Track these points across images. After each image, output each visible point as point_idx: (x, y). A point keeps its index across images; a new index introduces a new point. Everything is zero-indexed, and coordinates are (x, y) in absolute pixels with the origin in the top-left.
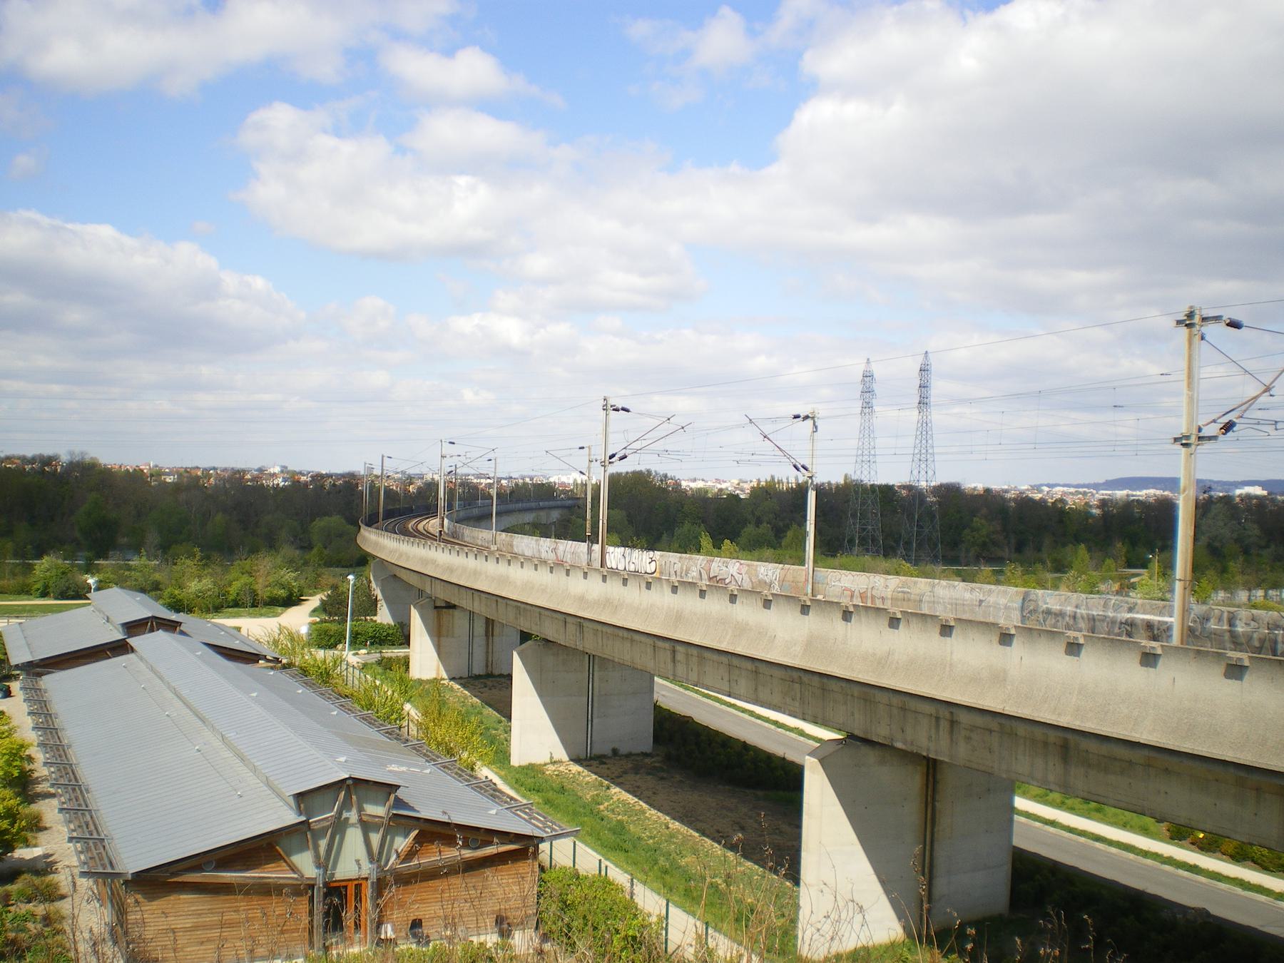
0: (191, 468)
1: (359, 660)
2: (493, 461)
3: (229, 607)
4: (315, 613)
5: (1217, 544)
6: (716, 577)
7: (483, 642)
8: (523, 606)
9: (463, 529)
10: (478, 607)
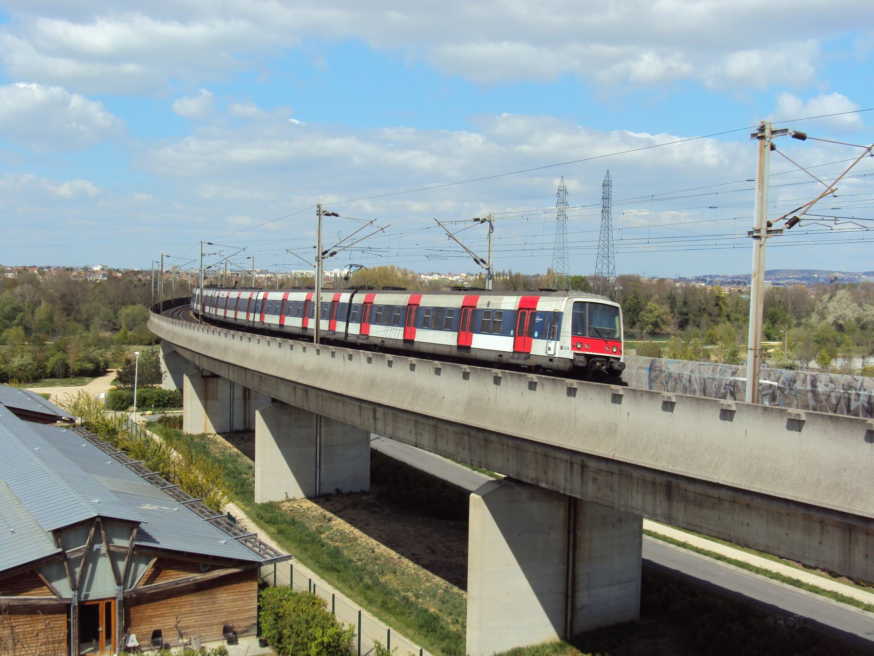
0: (29, 267)
1: (145, 419)
2: (252, 259)
3: (47, 378)
4: (116, 383)
5: (841, 322)
8: (263, 376)
10: (232, 376)
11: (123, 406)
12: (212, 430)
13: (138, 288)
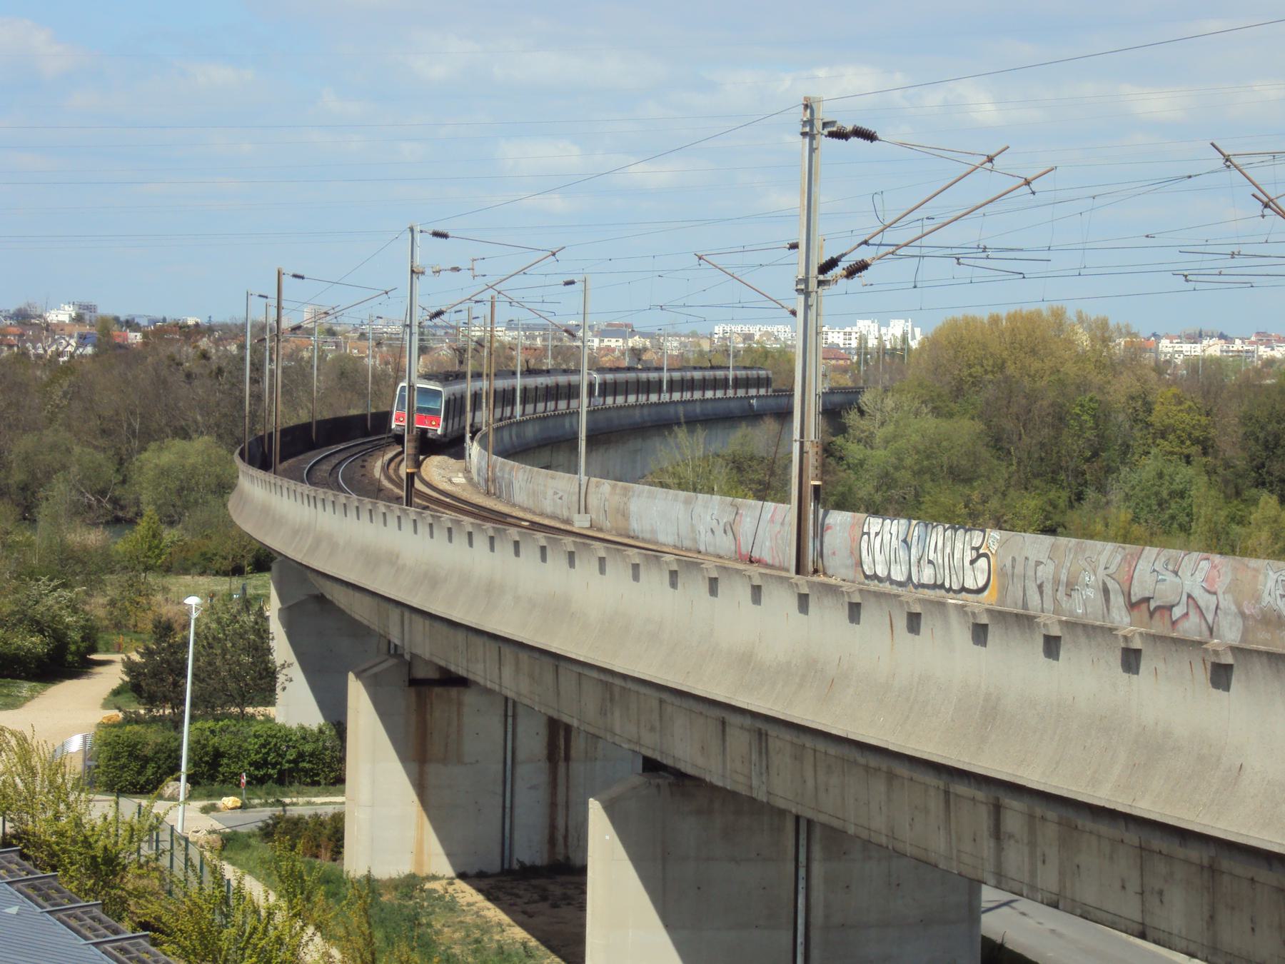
1: (218, 826)
2: (578, 286)
4: (121, 700)
6: (1147, 600)
7: (542, 778)
8: (618, 682)
9: (512, 469)
11: (142, 780)
12: (439, 864)
13: (196, 383)
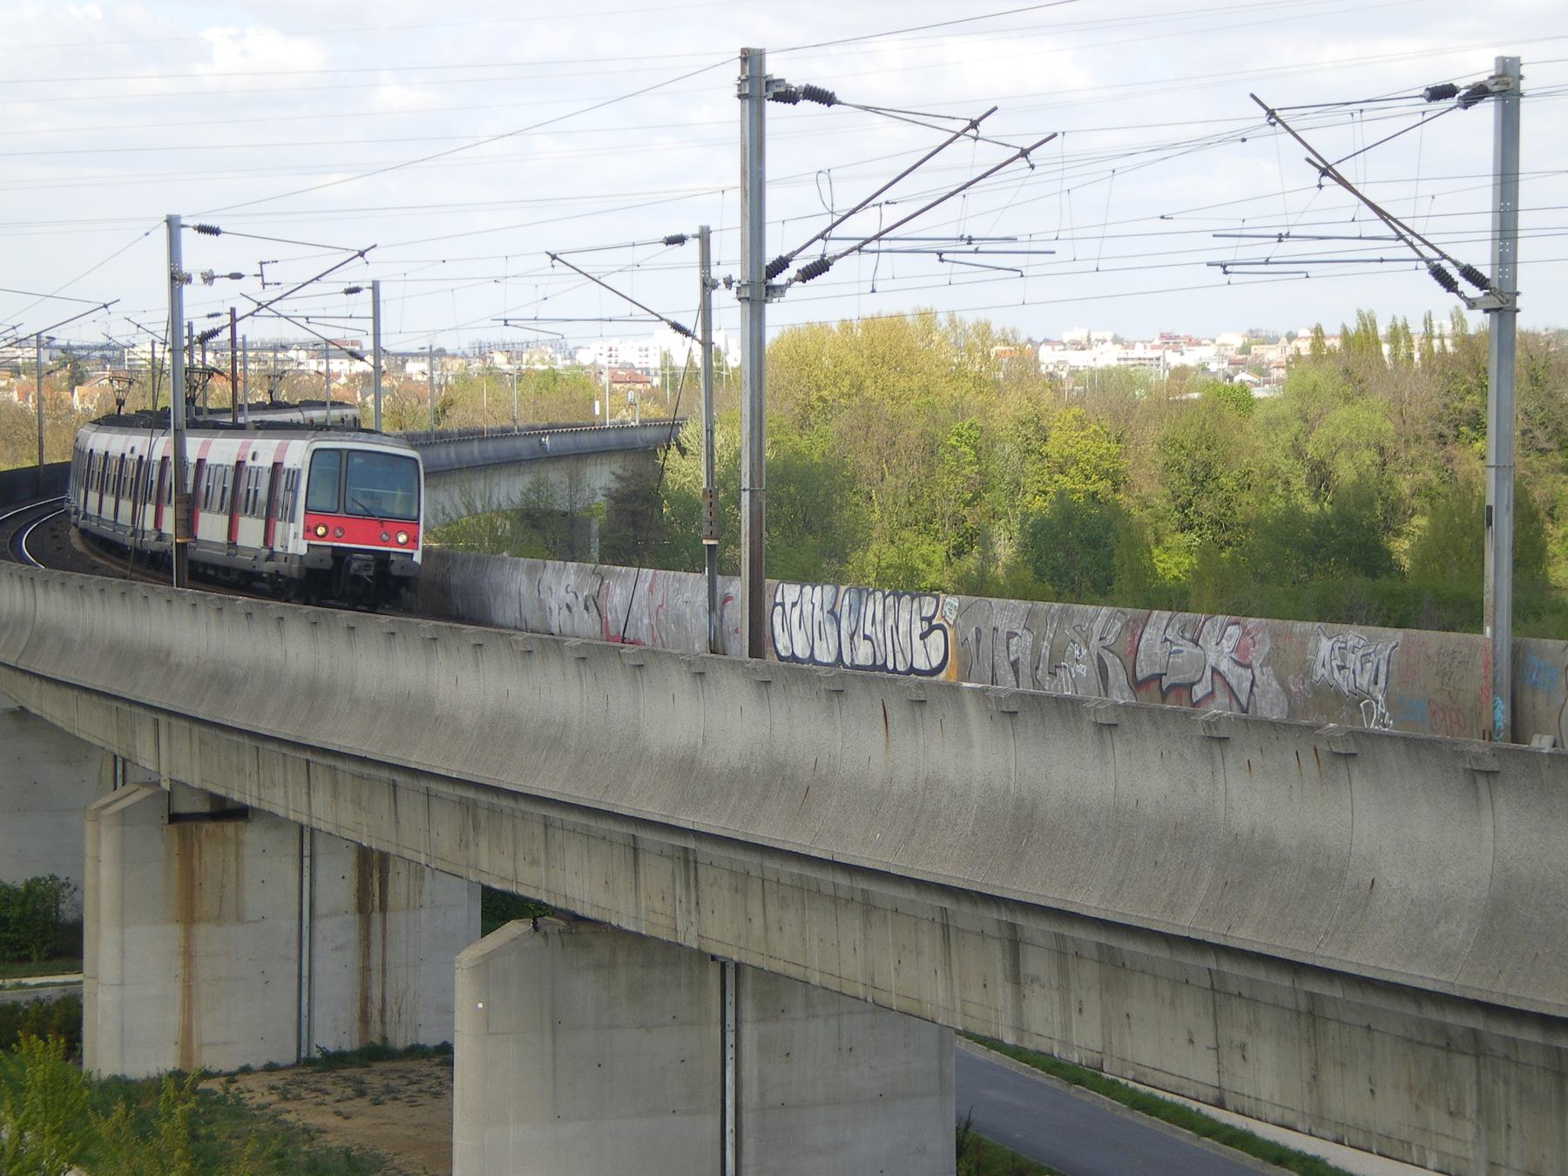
8: (483, 798)
